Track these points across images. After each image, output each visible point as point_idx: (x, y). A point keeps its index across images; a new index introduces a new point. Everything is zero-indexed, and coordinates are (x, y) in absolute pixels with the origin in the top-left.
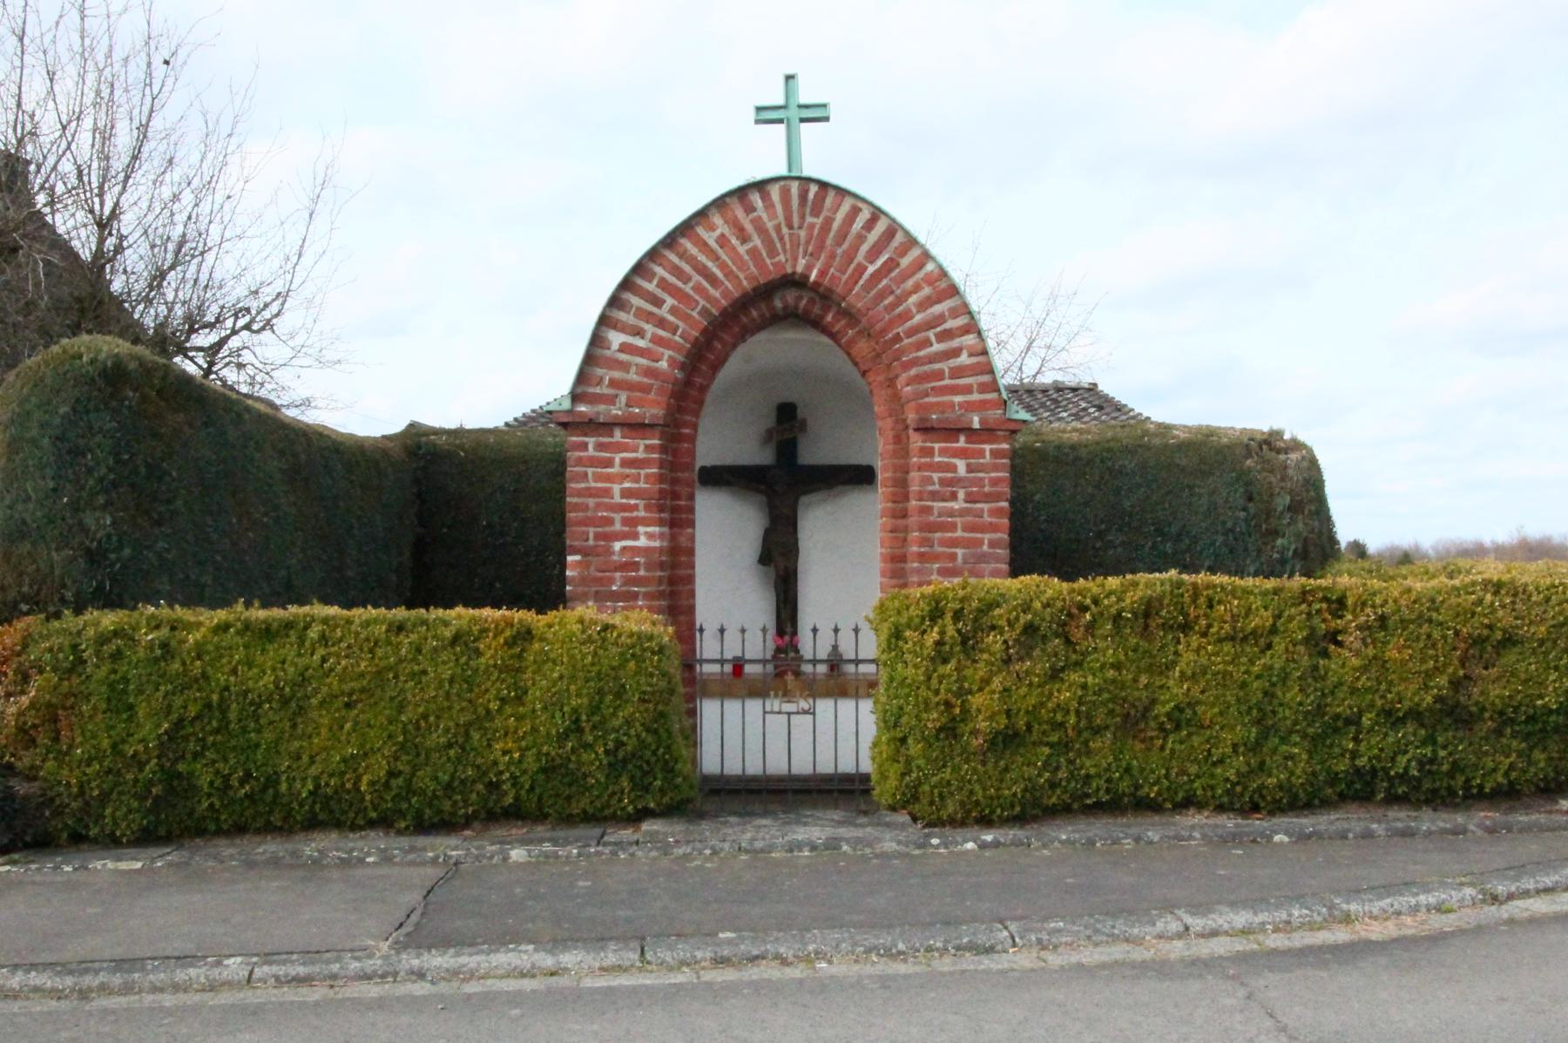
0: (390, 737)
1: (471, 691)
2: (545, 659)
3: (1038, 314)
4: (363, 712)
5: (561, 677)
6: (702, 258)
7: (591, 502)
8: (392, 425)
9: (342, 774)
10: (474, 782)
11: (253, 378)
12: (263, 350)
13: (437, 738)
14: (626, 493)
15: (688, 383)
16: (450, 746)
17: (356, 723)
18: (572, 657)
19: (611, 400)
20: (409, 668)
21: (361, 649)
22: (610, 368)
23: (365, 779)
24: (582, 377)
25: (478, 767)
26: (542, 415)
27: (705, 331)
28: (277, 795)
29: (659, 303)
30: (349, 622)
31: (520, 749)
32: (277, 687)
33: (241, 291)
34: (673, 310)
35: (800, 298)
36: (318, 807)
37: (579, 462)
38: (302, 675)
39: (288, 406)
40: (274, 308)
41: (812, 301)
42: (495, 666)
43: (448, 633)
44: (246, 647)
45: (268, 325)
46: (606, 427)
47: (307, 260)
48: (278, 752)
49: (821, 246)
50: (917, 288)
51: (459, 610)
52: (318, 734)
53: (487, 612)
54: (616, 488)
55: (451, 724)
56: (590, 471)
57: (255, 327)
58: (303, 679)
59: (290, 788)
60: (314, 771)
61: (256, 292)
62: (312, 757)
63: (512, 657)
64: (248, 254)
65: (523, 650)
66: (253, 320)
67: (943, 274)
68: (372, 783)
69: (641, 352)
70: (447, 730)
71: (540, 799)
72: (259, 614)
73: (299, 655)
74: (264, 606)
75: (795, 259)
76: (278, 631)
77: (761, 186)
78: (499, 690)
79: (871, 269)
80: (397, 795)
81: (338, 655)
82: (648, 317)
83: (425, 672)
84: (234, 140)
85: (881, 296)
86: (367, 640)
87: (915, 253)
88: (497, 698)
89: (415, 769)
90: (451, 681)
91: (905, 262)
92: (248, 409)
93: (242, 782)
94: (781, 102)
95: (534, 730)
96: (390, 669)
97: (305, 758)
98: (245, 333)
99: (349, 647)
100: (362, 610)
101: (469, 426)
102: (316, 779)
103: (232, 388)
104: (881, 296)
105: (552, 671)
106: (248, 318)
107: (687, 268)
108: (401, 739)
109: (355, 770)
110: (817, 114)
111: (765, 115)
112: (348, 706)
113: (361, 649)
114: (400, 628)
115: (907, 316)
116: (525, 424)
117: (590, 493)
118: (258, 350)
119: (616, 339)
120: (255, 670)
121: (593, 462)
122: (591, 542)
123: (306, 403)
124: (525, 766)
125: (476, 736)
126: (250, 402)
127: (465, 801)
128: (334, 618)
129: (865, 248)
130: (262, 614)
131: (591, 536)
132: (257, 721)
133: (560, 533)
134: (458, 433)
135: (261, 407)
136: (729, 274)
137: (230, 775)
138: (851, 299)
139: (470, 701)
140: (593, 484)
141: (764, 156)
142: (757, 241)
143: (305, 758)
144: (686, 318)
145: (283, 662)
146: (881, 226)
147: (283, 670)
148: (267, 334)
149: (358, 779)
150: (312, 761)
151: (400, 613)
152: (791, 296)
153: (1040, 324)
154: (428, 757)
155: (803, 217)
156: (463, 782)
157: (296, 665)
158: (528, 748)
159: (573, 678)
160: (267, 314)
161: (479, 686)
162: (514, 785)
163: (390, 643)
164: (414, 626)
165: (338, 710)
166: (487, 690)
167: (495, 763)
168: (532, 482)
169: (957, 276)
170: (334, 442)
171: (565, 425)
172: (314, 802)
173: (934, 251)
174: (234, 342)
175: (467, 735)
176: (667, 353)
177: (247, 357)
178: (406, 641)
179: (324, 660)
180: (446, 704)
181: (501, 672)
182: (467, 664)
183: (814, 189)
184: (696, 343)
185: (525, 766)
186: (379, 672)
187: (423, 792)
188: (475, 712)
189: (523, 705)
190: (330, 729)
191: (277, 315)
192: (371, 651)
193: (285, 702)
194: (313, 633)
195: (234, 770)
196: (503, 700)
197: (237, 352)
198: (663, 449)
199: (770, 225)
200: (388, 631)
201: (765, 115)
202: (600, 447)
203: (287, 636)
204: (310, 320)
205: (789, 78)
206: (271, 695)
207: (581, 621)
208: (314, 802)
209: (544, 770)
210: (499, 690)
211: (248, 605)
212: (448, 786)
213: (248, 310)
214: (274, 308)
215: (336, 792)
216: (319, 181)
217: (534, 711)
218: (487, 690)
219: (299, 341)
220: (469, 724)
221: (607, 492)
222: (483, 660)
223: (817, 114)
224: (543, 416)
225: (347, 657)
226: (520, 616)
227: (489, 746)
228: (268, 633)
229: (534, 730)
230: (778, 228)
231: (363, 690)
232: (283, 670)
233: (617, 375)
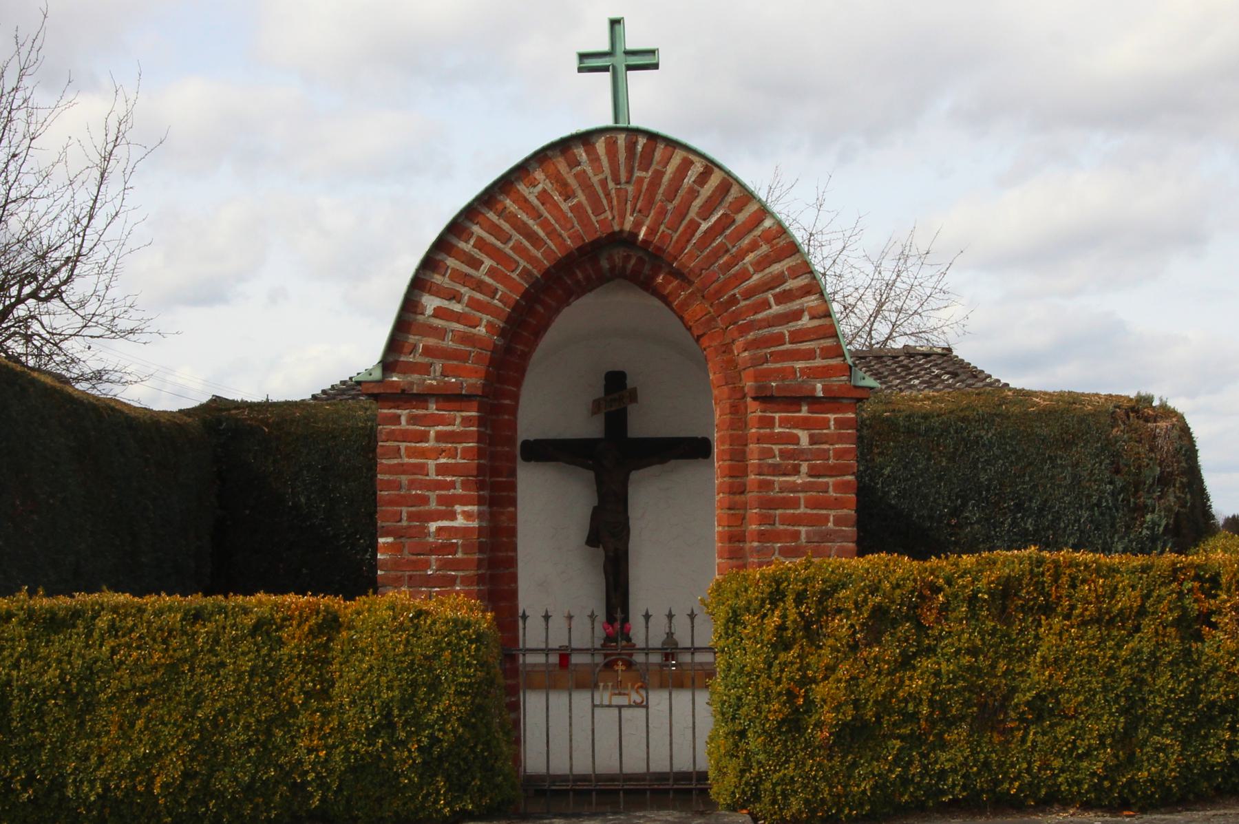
0: (185, 735)
1: (273, 684)
2: (354, 648)
3: (888, 275)
4: (156, 708)
5: (371, 669)
6: (522, 216)
7: (404, 479)
8: (195, 397)
9: (133, 776)
10: (277, 783)
11: (40, 349)
12: (56, 317)
13: (236, 736)
14: (441, 469)
15: (508, 350)
16: (250, 744)
17: (149, 720)
18: (382, 647)
19: (425, 369)
20: (204, 659)
21: (154, 640)
22: (423, 335)
23: (158, 782)
24: (395, 344)
25: (281, 766)
26: (351, 388)
27: (526, 295)
28: (64, 798)
29: (476, 264)
30: (141, 610)
31: (326, 747)
32: (63, 680)
33: (26, 257)
34: (492, 272)
35: (627, 259)
36: (107, 811)
37: (392, 436)
38: (90, 668)
39: (77, 380)
40: (63, 274)
41: (641, 261)
42: (299, 656)
43: (249, 621)
44: (29, 638)
45: (57, 293)
46: (421, 398)
47: (99, 222)
48: (64, 752)
49: (650, 201)
50: (754, 246)
51: (261, 596)
52: (108, 733)
53: (290, 598)
54: (431, 464)
55: (252, 720)
56: (403, 445)
57: (43, 294)
58: (90, 673)
59: (77, 790)
60: (101, 773)
61: (43, 257)
62: (100, 757)
63: (317, 647)
64: (35, 217)
65: (329, 640)
66: (40, 288)
67: (782, 230)
68: (165, 786)
69: (457, 317)
70: (247, 727)
71: (348, 800)
72: (43, 602)
73: (87, 646)
74: (50, 594)
75: (623, 217)
76: (64, 620)
77: (586, 138)
78: (303, 684)
79: (704, 226)
80: (193, 798)
81: (129, 646)
82: (465, 279)
83: (222, 664)
84: (20, 95)
85: (716, 254)
86: (161, 629)
87: (752, 208)
88: (301, 690)
89: (212, 770)
90: (252, 673)
91: (741, 218)
92: (33, 382)
93: (26, 785)
94: (606, 47)
95: (342, 725)
96: (184, 660)
97: (94, 759)
98: (31, 302)
99: (140, 638)
100: (154, 598)
101: (275, 398)
102: (105, 782)
103: (16, 359)
104: (716, 254)
105: (361, 661)
106: (34, 285)
107: (506, 226)
108: (197, 737)
109: (148, 771)
110: (646, 60)
111: (588, 62)
112: (141, 702)
113: (154, 640)
114: (198, 616)
115: (745, 275)
116: (334, 397)
117: (403, 469)
118: (45, 319)
119: (430, 303)
120: (39, 663)
121: (406, 436)
122: (404, 523)
123: (98, 376)
124: (331, 766)
125: (279, 733)
126: (35, 374)
127: (267, 804)
128: (124, 606)
129: (697, 203)
130: (46, 602)
131: (404, 516)
132: (41, 720)
133: (372, 515)
134: (266, 406)
135: (49, 380)
136: (551, 233)
137: (12, 777)
138: (683, 258)
139: (272, 696)
140: (406, 460)
141: (586, 106)
142: (581, 197)
143: (94, 759)
144: (504, 279)
145: (70, 655)
146: (715, 180)
147: (69, 662)
148: (55, 304)
149: (151, 780)
150: (101, 762)
151: (197, 600)
152: (619, 254)
153: (890, 286)
154: (226, 758)
155: (630, 172)
156: (264, 783)
157: (83, 657)
158: (334, 747)
159: (383, 669)
160: (55, 281)
161: (282, 679)
162: (320, 787)
163: (185, 633)
164: (211, 614)
165: (130, 706)
166: (290, 684)
167: (300, 762)
168: (341, 458)
169: (799, 236)
170: (127, 417)
171: (376, 397)
172: (104, 807)
173: (775, 208)
174: (21, 311)
175: (269, 734)
176: (486, 318)
177: (35, 327)
178: (202, 632)
179: (114, 651)
180: (246, 698)
181: (305, 663)
182: (269, 655)
183: (642, 141)
184: (516, 307)
185: (331, 766)
186: (173, 665)
187: (220, 795)
188: (278, 707)
189: (331, 699)
190: (121, 728)
191: (65, 282)
192: (164, 641)
193: (71, 698)
194: (102, 623)
195: (15, 773)
196: (308, 695)
197: (25, 321)
198: (481, 422)
199: (595, 180)
200: (183, 619)
201: (588, 62)
202: (413, 420)
203: (74, 626)
204: (101, 287)
205: (615, 23)
206: (56, 690)
207: (392, 608)
208: (104, 807)
209: (352, 769)
210: (303, 684)
211: (32, 593)
212: (249, 788)
213: (34, 277)
214: (63, 274)
215: (127, 795)
216: (112, 137)
217: (341, 705)
218: (290, 684)
219: (90, 309)
220: (271, 721)
221: (422, 469)
222: (285, 650)
223: (646, 60)
224: (350, 390)
225: (139, 648)
226: (324, 601)
227: (293, 744)
228: (54, 623)
229: (342, 725)
230: (604, 183)
231: (155, 684)
232: (69, 662)
233: (431, 341)
